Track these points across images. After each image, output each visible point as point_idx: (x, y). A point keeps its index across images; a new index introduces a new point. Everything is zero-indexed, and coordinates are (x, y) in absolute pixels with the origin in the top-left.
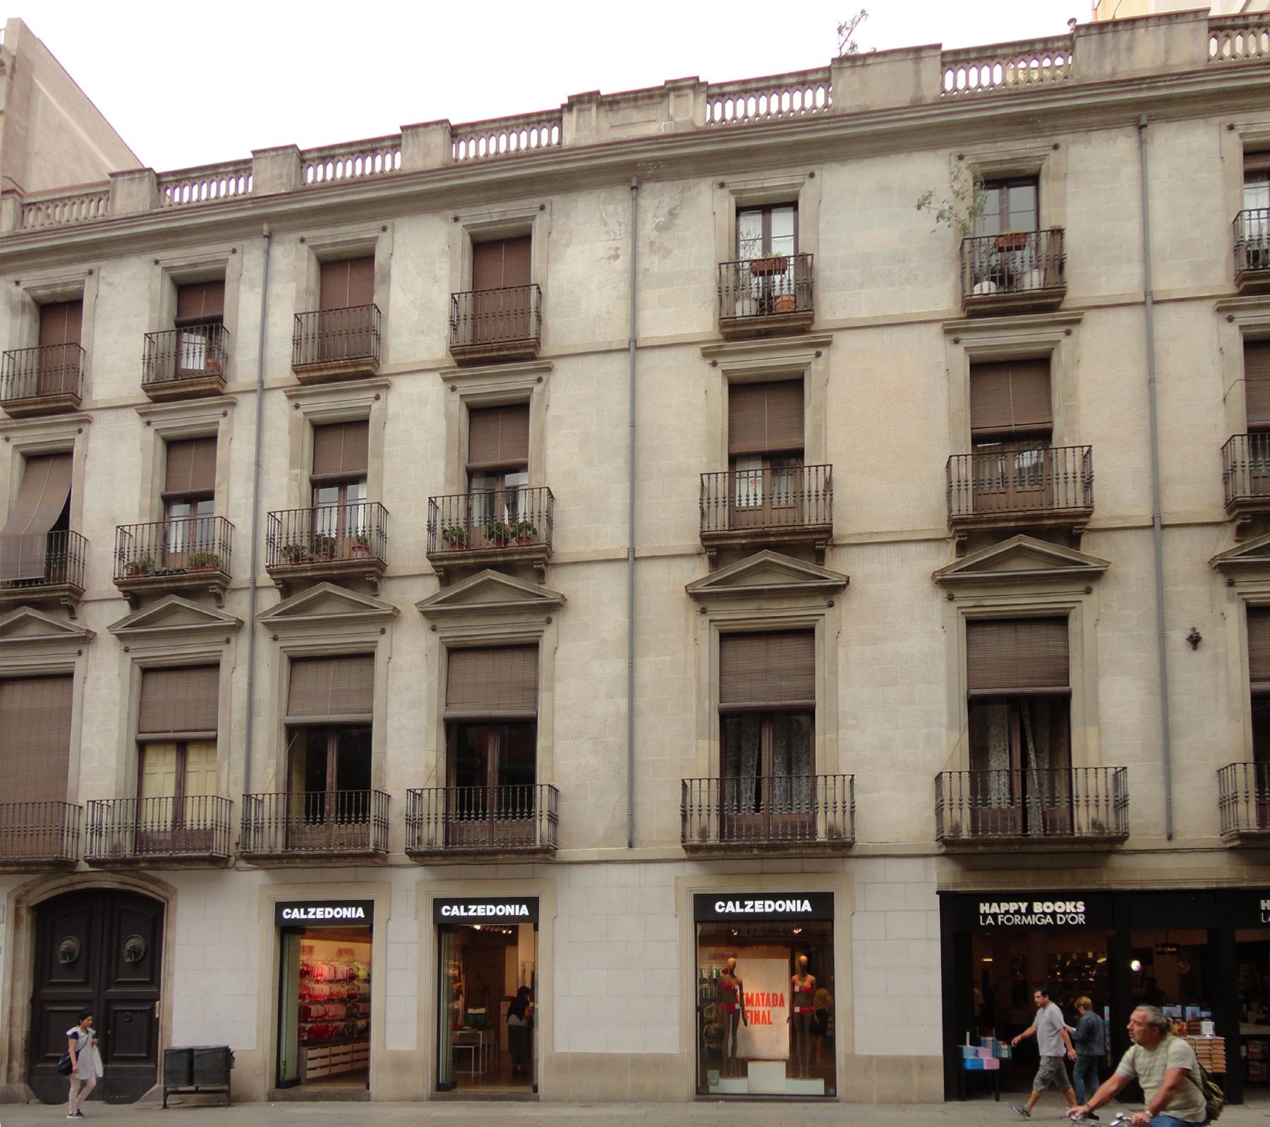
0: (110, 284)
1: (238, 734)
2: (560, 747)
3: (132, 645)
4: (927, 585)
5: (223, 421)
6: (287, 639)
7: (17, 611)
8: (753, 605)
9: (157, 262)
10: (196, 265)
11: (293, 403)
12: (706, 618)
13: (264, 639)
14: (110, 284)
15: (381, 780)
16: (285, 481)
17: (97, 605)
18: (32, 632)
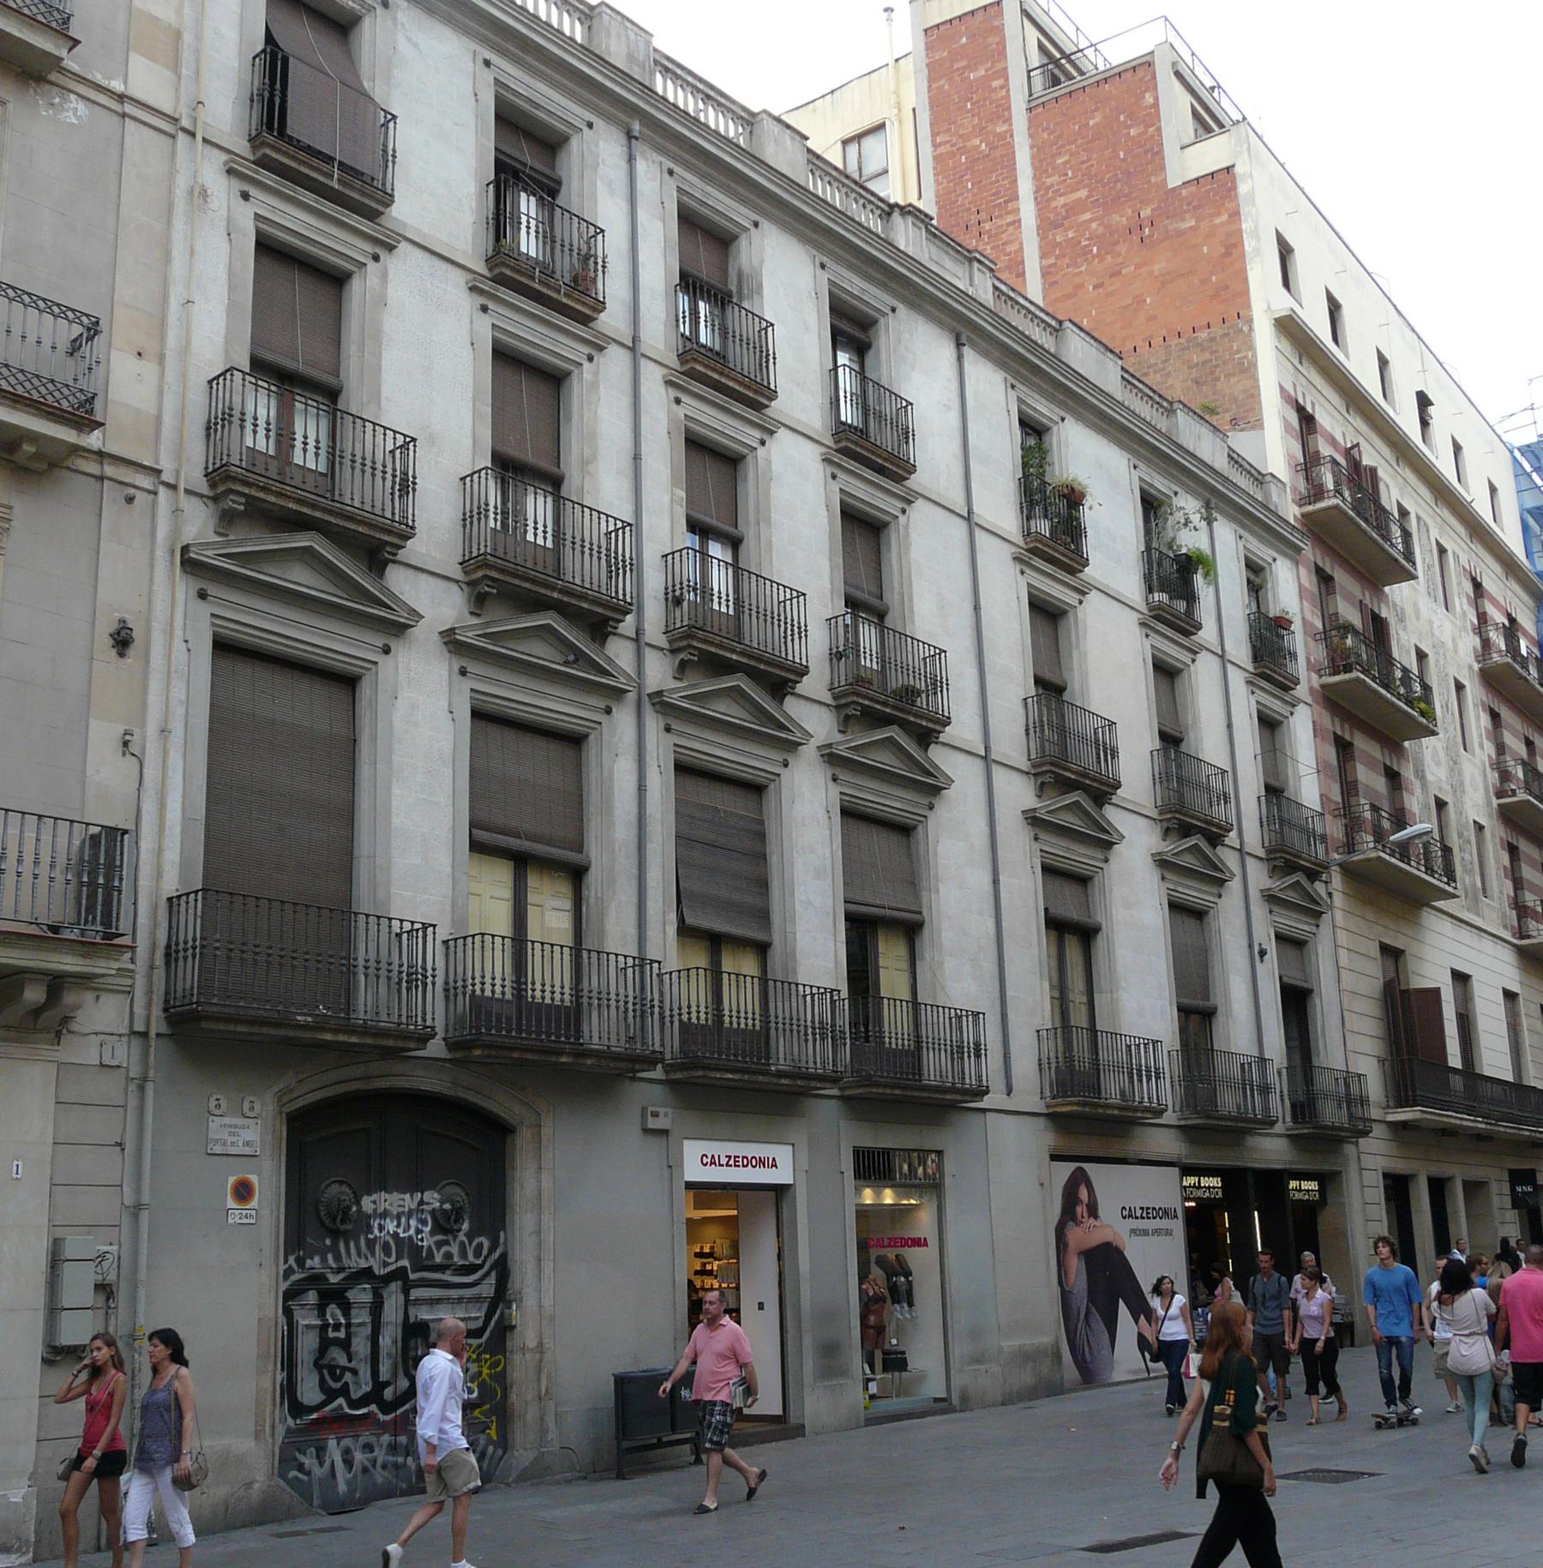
0: (416, 45)
1: (625, 863)
2: (950, 964)
3: (472, 667)
4: (1150, 860)
5: (586, 364)
6: (681, 734)
7: (299, 535)
8: (1063, 842)
9: (487, 63)
10: (538, 106)
11: (673, 393)
12: (1037, 846)
13: (653, 724)
14: (416, 45)
15: (795, 973)
16: (666, 498)
17: (410, 572)
18: (301, 578)
